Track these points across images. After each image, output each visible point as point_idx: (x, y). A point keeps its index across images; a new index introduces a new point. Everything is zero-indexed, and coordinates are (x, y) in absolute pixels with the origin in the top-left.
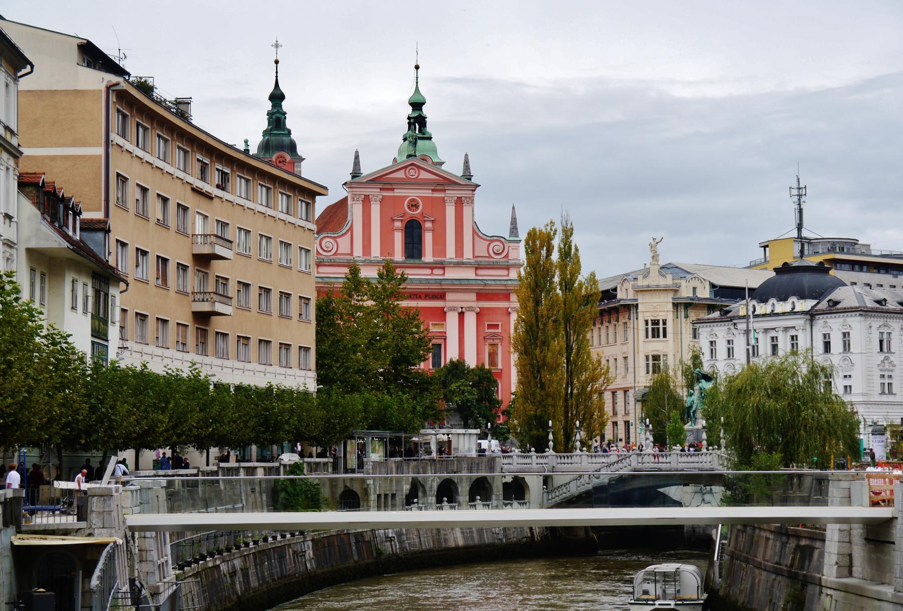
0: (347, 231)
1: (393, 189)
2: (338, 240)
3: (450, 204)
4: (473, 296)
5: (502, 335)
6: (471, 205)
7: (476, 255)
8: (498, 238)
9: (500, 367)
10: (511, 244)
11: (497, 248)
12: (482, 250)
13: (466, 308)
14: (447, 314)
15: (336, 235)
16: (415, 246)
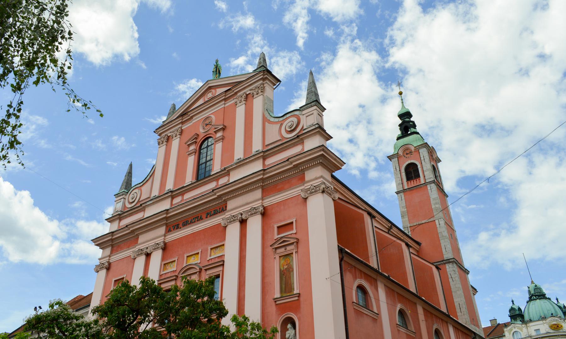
0: (151, 176)
1: (192, 117)
2: (143, 188)
3: (240, 104)
4: (258, 194)
5: (297, 236)
6: (261, 93)
7: (266, 144)
8: (292, 114)
9: (296, 291)
10: (304, 112)
11: (289, 124)
12: (273, 135)
13: (247, 212)
14: (228, 229)
15: (142, 184)
16: (208, 164)
